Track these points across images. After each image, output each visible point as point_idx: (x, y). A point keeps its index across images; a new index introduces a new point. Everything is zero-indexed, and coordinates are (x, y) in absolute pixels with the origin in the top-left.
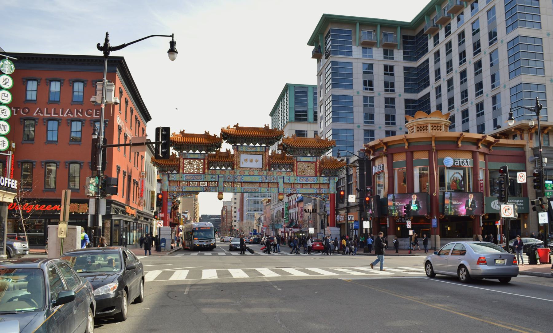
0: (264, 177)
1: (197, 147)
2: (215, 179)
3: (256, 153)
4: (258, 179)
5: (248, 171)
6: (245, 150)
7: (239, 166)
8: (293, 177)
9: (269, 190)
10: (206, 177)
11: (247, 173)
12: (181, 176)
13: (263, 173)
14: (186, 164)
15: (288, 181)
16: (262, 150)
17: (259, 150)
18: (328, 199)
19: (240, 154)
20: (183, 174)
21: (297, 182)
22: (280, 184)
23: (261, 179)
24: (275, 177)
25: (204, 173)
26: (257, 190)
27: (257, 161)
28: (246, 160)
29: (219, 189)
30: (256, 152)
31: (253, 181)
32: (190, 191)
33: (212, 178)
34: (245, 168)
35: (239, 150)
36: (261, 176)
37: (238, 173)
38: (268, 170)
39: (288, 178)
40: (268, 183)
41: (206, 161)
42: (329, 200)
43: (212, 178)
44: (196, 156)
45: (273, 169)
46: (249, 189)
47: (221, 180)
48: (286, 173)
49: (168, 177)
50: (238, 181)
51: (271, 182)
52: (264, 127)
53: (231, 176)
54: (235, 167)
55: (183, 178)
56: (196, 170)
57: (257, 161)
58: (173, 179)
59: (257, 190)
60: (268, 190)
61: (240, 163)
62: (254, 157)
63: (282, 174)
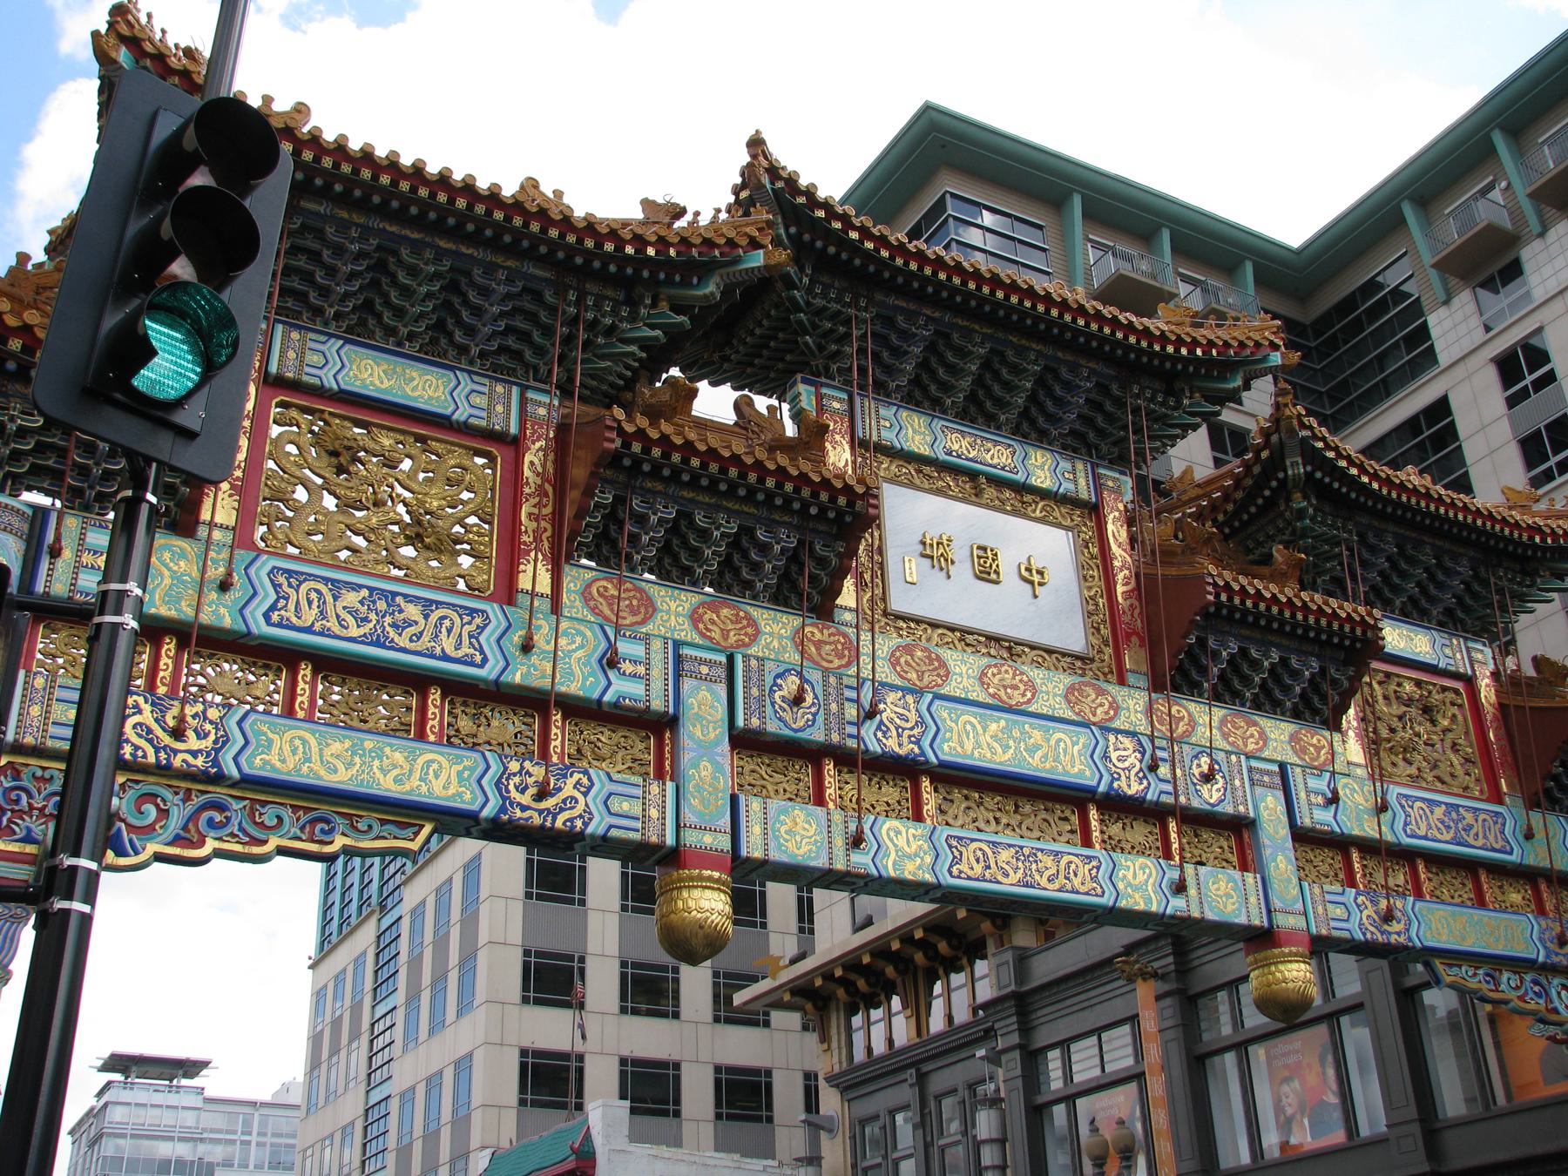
0: (1127, 742)
9: (1192, 891)
10: (542, 639)
12: (216, 572)
14: (291, 449)
15: (1323, 818)
16: (1067, 487)
20: (243, 556)
23: (1106, 757)
27: (1032, 577)
28: (935, 553)
29: (689, 817)
33: (611, 661)
34: (934, 625)
36: (1106, 730)
39: (1320, 784)
41: (533, 458)
50: (892, 744)
53: (814, 676)
54: (848, 596)
55: (237, 594)
56: (408, 551)
59: (1084, 870)
60: (1180, 888)
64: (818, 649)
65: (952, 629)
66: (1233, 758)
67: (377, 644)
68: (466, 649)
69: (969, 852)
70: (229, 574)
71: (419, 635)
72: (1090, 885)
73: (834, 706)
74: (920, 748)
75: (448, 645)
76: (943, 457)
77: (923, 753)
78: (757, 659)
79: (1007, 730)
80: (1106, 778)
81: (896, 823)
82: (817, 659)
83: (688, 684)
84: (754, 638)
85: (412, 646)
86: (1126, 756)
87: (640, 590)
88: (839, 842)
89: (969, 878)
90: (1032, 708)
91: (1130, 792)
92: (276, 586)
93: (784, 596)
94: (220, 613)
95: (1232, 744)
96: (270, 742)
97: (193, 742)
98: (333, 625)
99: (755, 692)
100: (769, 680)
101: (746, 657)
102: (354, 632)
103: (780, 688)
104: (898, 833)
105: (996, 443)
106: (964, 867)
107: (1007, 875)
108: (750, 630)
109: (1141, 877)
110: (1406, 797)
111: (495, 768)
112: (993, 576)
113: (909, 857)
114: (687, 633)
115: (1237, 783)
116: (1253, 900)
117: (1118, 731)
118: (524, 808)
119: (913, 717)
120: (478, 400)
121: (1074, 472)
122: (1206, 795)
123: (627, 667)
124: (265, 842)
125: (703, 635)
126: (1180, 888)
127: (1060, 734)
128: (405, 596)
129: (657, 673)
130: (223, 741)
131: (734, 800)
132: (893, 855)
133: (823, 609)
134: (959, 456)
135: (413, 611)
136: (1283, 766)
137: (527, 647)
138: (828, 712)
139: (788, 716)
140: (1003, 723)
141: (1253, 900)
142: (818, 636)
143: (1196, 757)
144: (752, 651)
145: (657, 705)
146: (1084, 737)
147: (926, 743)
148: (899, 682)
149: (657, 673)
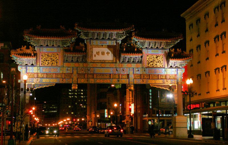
1: (53, 41)
22: (130, 76)
28: (98, 53)
33: (68, 70)
39: (137, 69)
42: (177, 90)
80: (112, 72)
97: (38, 81)
114: (74, 66)
136: (133, 68)
137: (61, 70)
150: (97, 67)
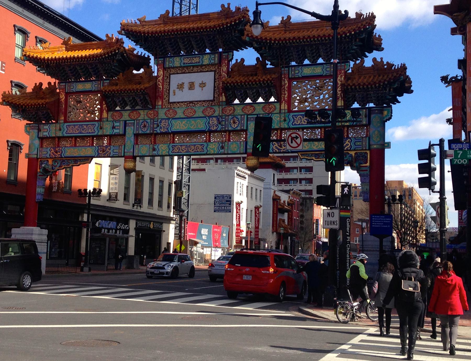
0: (214, 119)
2: (119, 129)
3: (201, 68)
4: (201, 125)
5: (183, 110)
6: (179, 65)
7: (167, 99)
8: (278, 115)
9: (226, 148)
11: (180, 114)
13: (214, 111)
17: (206, 62)
18: (366, 163)
19: (170, 74)
21: (286, 126)
23: (209, 123)
24: (239, 117)
25: (101, 120)
26: (200, 147)
27: (203, 85)
28: (181, 86)
29: (126, 151)
30: (202, 66)
31: (193, 128)
32: (75, 155)
33: (114, 127)
34: (178, 103)
35: (167, 66)
36: (210, 117)
37: (162, 114)
38: (224, 103)
40: (225, 131)
43: (114, 127)
44: (88, 86)
45: (237, 101)
46: (183, 147)
47: (130, 131)
48: (263, 107)
49: (39, 130)
50: (162, 130)
51: (230, 129)
52: (219, 9)
53: (149, 121)
56: (89, 115)
57: (203, 85)
58: (46, 134)
59: (200, 147)
61: (169, 93)
62: (197, 78)
63: (254, 109)
64: (151, 115)
65: (182, 102)
66: (243, 116)
67: (81, 133)
68: (93, 131)
69: (176, 148)
70: (60, 128)
71: (86, 130)
72: (201, 150)
73: (152, 126)
74: (168, 130)
75: (90, 131)
76: (182, 65)
77: (168, 131)
78: (140, 120)
79: (187, 122)
80: (208, 127)
81: (162, 145)
82: (151, 117)
83: (127, 128)
84: (139, 117)
85: (85, 132)
86: (215, 121)
87: (120, 113)
88: (151, 150)
89: (175, 153)
90: (194, 116)
91: (213, 130)
92: (67, 128)
93: (145, 107)
94: (60, 134)
95: (245, 113)
96: (67, 151)
98: (74, 132)
99: (138, 126)
100: (140, 124)
101: (136, 120)
102: (77, 132)
103: (142, 125)
104: (162, 146)
105: (195, 57)
106: (175, 151)
107: (183, 151)
108: (139, 115)
109: (214, 147)
110: (295, 115)
111: (97, 149)
112: (193, 88)
113: (164, 151)
114: (128, 118)
115: (242, 122)
116: (242, 147)
117: (214, 117)
118: (101, 154)
119: (167, 124)
120: (96, 86)
121: (215, 58)
122: (233, 126)
123: (116, 128)
124: (69, 165)
125: (130, 118)
126: (222, 148)
127: (198, 120)
128: (84, 124)
129: (121, 127)
130: (62, 152)
131: (134, 146)
132: (161, 151)
133: (154, 107)
134: (186, 64)
135: (85, 127)
138: (151, 127)
139: (143, 130)
140: (186, 121)
141: (242, 147)
142: (151, 112)
143: (232, 118)
144: (139, 119)
145: (121, 133)
146: (205, 120)
147: (169, 129)
148: (166, 117)
149: (121, 127)
150: (176, 117)
